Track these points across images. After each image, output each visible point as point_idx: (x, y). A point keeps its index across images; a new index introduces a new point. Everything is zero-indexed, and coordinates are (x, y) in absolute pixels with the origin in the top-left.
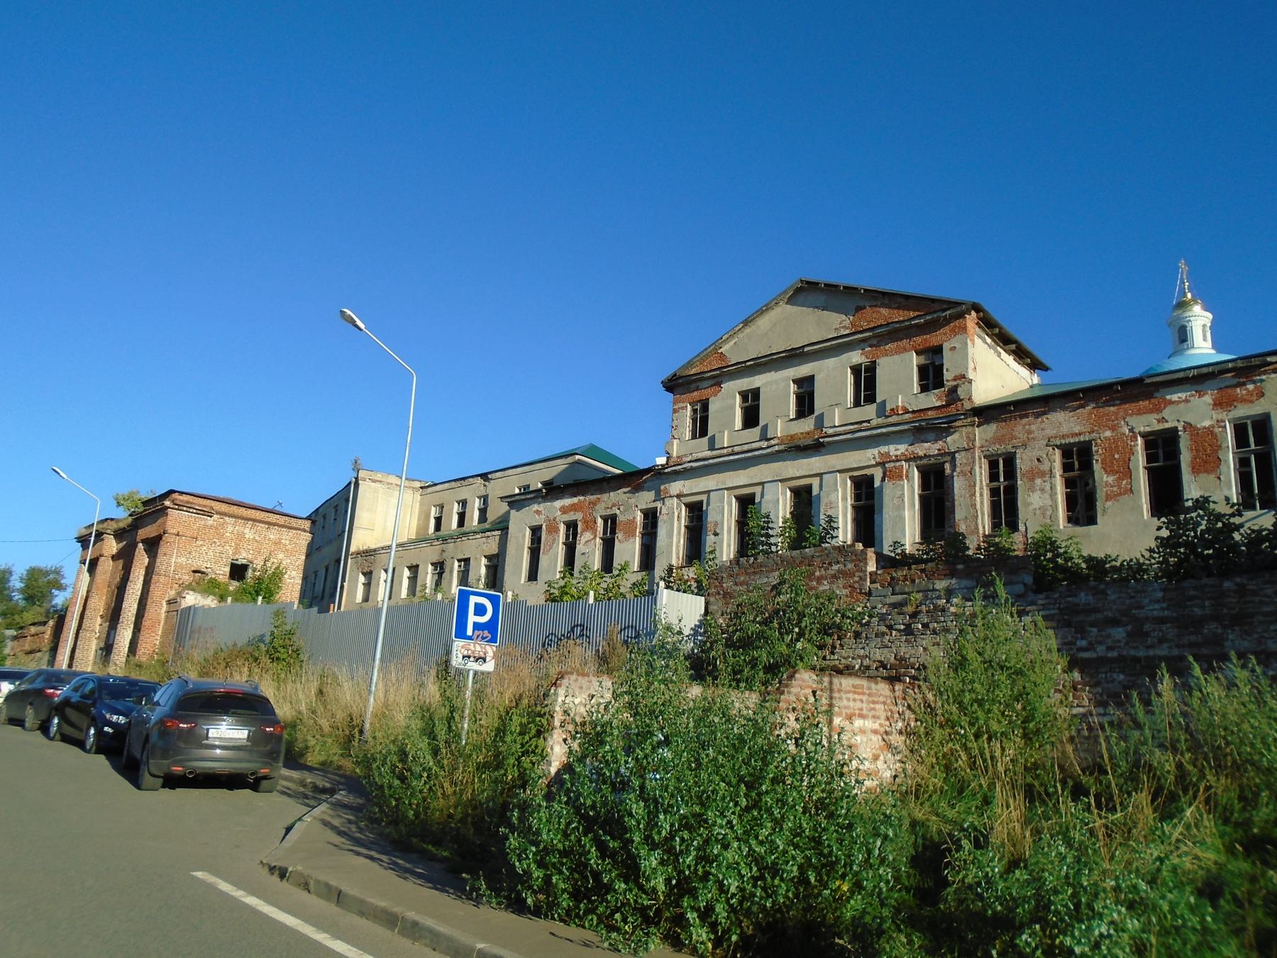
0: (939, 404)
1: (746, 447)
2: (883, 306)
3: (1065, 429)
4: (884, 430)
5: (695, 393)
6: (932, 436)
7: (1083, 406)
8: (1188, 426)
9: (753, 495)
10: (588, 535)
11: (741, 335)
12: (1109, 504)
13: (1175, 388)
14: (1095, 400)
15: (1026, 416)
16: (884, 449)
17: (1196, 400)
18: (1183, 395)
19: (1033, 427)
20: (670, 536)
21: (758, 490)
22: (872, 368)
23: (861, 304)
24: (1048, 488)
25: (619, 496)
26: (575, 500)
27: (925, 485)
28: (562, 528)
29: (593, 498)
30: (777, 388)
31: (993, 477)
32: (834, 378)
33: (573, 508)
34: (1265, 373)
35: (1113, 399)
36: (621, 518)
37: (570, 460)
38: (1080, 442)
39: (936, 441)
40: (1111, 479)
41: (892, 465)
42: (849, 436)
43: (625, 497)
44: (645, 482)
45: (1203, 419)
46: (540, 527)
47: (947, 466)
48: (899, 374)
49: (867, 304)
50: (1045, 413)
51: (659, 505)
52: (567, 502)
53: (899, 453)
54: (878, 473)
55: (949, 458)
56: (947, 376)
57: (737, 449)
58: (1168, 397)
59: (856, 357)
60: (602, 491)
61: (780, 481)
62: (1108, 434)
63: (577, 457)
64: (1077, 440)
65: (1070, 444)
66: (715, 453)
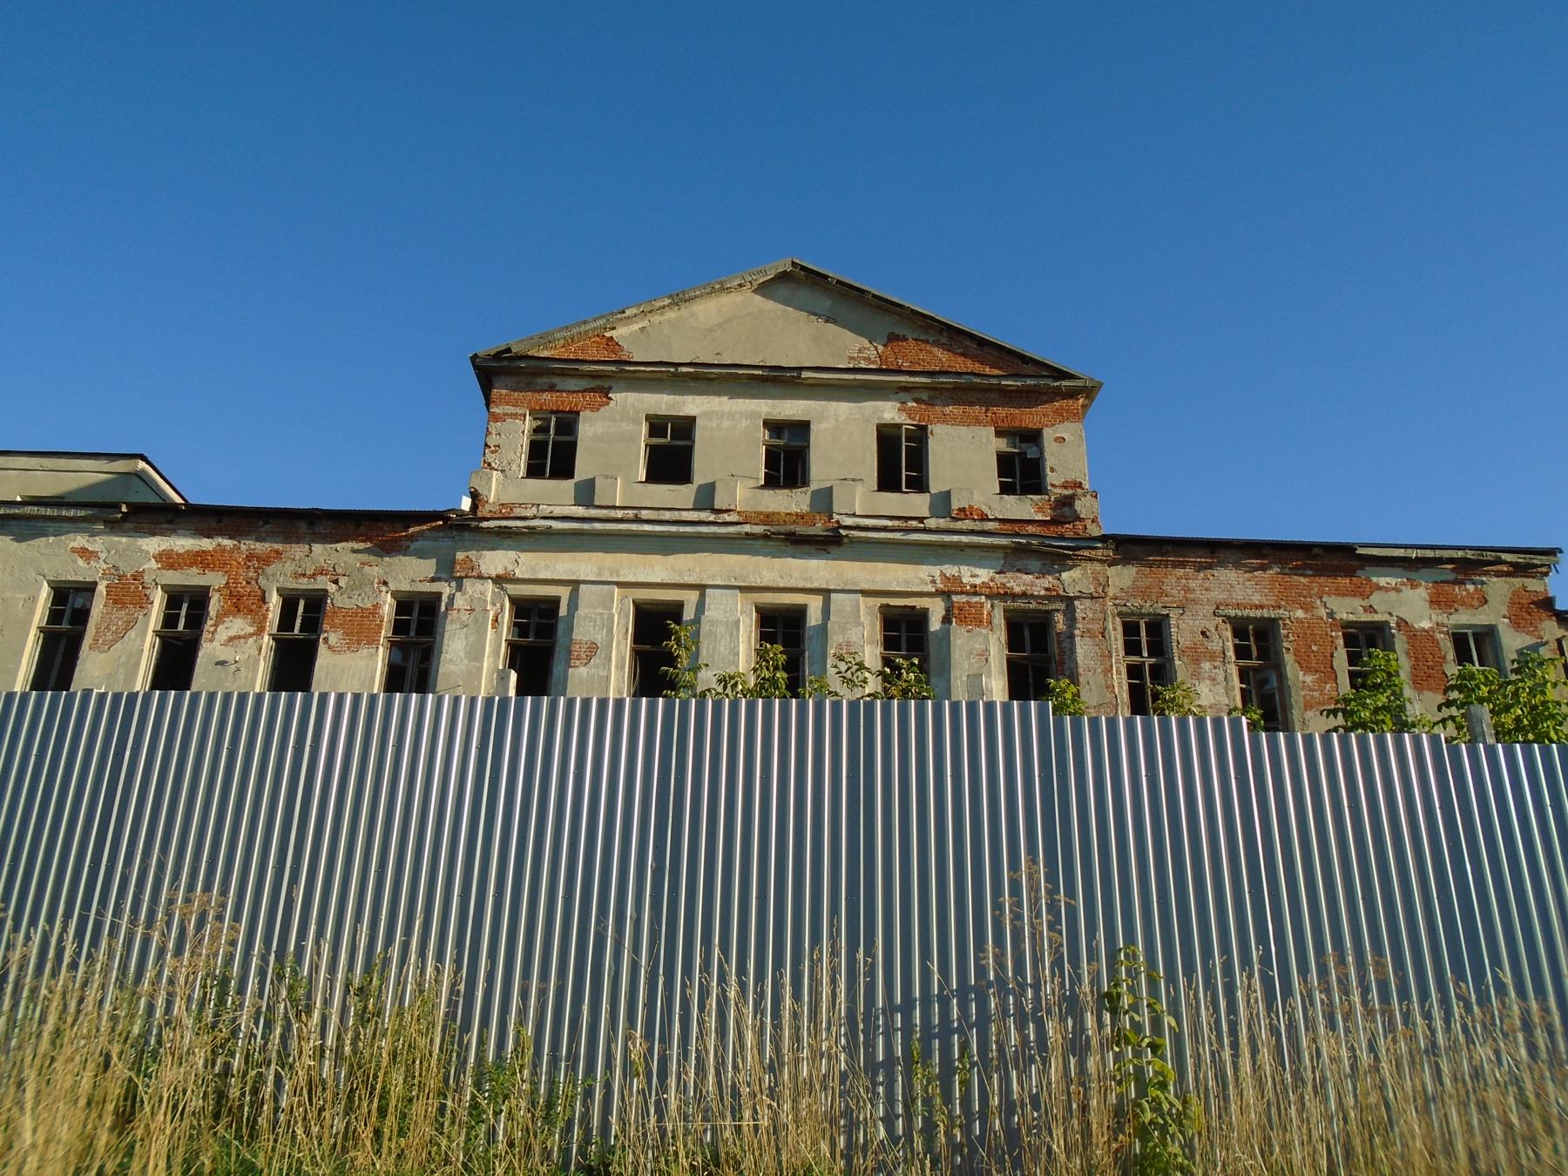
0: (1039, 517)
1: (667, 516)
2: (936, 344)
3: (1239, 596)
4: (964, 539)
5: (547, 396)
6: (1035, 564)
7: (1263, 568)
8: (1402, 623)
9: (680, 606)
10: (238, 625)
11: (656, 318)
12: (1309, 714)
13: (1386, 570)
14: (1280, 562)
15: (1182, 565)
16: (951, 570)
17: (1408, 592)
18: (1393, 581)
19: (1192, 584)
20: (476, 654)
21: (690, 598)
22: (920, 436)
23: (899, 331)
24: (1221, 678)
25: (344, 554)
26: (207, 544)
27: (1014, 642)
28: (158, 599)
29: (260, 547)
30: (730, 430)
31: (1132, 648)
32: (844, 435)
33: (200, 560)
34: (1487, 573)
35: (1305, 567)
36: (339, 600)
37: (121, 466)
38: (1262, 619)
39: (1043, 574)
40: (1309, 679)
41: (964, 598)
42: (898, 536)
43: (355, 560)
44: (412, 538)
45: (1421, 618)
46: (90, 588)
47: (1059, 617)
48: (964, 455)
49: (910, 336)
50: (1210, 567)
51: (446, 589)
52: (183, 543)
53: (978, 581)
54: (936, 609)
55: (1062, 606)
56: (1051, 478)
57: (645, 514)
58: (1374, 579)
59: (890, 412)
60: (290, 537)
61: (741, 589)
62: (1300, 614)
63: (142, 465)
64: (1258, 613)
65: (1248, 618)
66: (593, 513)
